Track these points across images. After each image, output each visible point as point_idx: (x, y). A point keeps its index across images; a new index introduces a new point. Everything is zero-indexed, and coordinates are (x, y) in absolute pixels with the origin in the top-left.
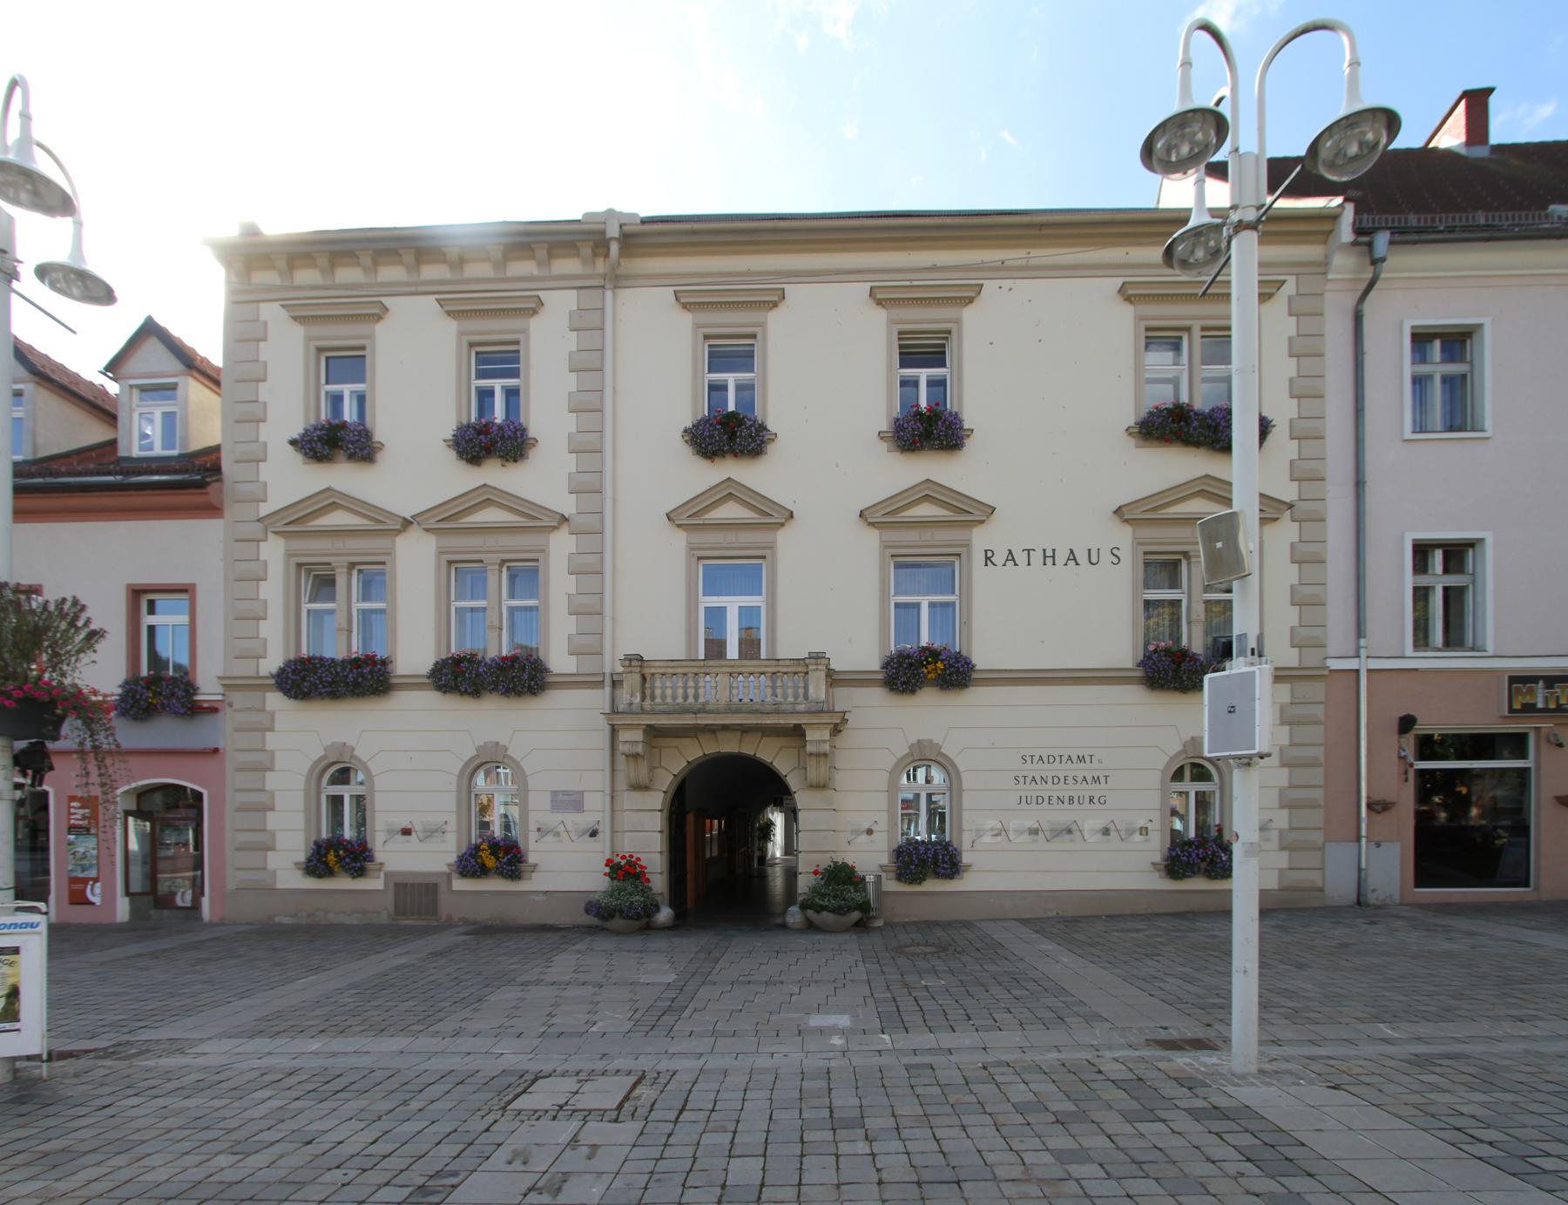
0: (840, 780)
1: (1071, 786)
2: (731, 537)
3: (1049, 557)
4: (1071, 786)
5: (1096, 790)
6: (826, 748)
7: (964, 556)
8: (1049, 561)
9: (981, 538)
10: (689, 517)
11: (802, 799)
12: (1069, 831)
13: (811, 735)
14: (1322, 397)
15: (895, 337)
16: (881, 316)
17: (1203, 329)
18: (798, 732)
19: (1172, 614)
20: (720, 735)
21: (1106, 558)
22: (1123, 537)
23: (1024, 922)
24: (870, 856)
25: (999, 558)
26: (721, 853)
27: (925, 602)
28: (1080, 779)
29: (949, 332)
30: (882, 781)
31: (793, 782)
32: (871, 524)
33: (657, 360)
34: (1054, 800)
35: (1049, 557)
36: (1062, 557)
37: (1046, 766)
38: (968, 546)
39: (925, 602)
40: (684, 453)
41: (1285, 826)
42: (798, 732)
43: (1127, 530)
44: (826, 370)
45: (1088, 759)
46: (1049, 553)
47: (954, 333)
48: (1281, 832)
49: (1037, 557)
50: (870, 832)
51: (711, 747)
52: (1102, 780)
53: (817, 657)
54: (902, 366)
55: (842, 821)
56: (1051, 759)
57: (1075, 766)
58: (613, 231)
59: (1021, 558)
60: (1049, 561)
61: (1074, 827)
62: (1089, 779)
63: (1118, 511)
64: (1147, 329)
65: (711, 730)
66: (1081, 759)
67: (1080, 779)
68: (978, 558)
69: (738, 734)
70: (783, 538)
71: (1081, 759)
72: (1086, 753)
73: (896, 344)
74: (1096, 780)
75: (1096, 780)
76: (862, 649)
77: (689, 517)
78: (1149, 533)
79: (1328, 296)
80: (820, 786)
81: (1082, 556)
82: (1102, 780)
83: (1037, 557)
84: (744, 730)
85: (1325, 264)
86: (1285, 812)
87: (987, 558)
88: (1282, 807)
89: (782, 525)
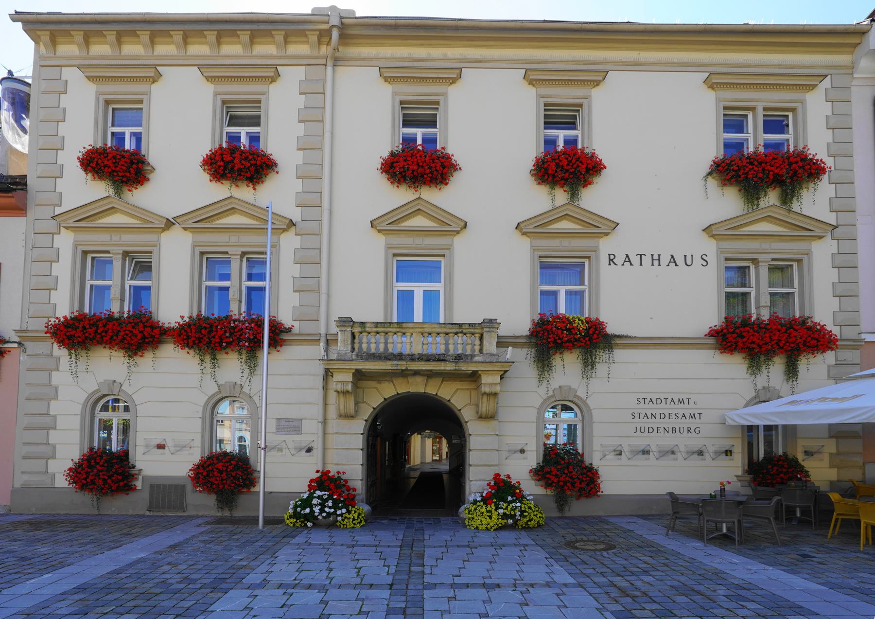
0: (502, 414)
1: (674, 420)
2: (418, 241)
3: (656, 260)
4: (674, 420)
5: (693, 424)
6: (497, 389)
7: (593, 259)
8: (656, 263)
9: (606, 246)
10: (387, 224)
11: (474, 429)
12: (673, 453)
13: (485, 379)
14: (851, 156)
15: (542, 108)
16: (531, 92)
17: (765, 109)
18: (474, 377)
19: (743, 300)
20: (411, 379)
21: (698, 261)
22: (710, 247)
23: (638, 516)
24: (521, 470)
25: (619, 260)
26: (408, 468)
27: (562, 290)
28: (680, 416)
29: (581, 105)
30: (532, 415)
31: (467, 414)
32: (524, 234)
33: (366, 118)
34: (662, 430)
35: (656, 260)
36: (665, 260)
37: (655, 406)
38: (596, 250)
39: (562, 290)
40: (382, 181)
41: (834, 450)
42: (474, 377)
43: (713, 243)
44: (492, 129)
45: (686, 401)
46: (656, 257)
47: (585, 106)
48: (831, 454)
49: (647, 260)
50: (522, 451)
51: (403, 387)
52: (697, 416)
53: (491, 323)
54: (545, 128)
55: (506, 444)
56: (659, 401)
57: (676, 406)
58: (335, 21)
59: (635, 260)
60: (656, 263)
61: (675, 449)
62: (687, 416)
63: (707, 230)
64: (725, 108)
65: (404, 374)
66: (681, 401)
67: (680, 416)
68: (604, 260)
69: (425, 378)
70: (458, 242)
71: (681, 401)
72: (685, 397)
73: (542, 113)
74: (692, 416)
75: (692, 416)
76: (519, 319)
77: (387, 224)
78: (728, 245)
79: (852, 88)
80: (490, 417)
81: (680, 260)
82: (697, 416)
83: (647, 260)
84: (430, 375)
85: (851, 68)
86: (834, 441)
87: (610, 260)
88: (831, 437)
89: (458, 232)
